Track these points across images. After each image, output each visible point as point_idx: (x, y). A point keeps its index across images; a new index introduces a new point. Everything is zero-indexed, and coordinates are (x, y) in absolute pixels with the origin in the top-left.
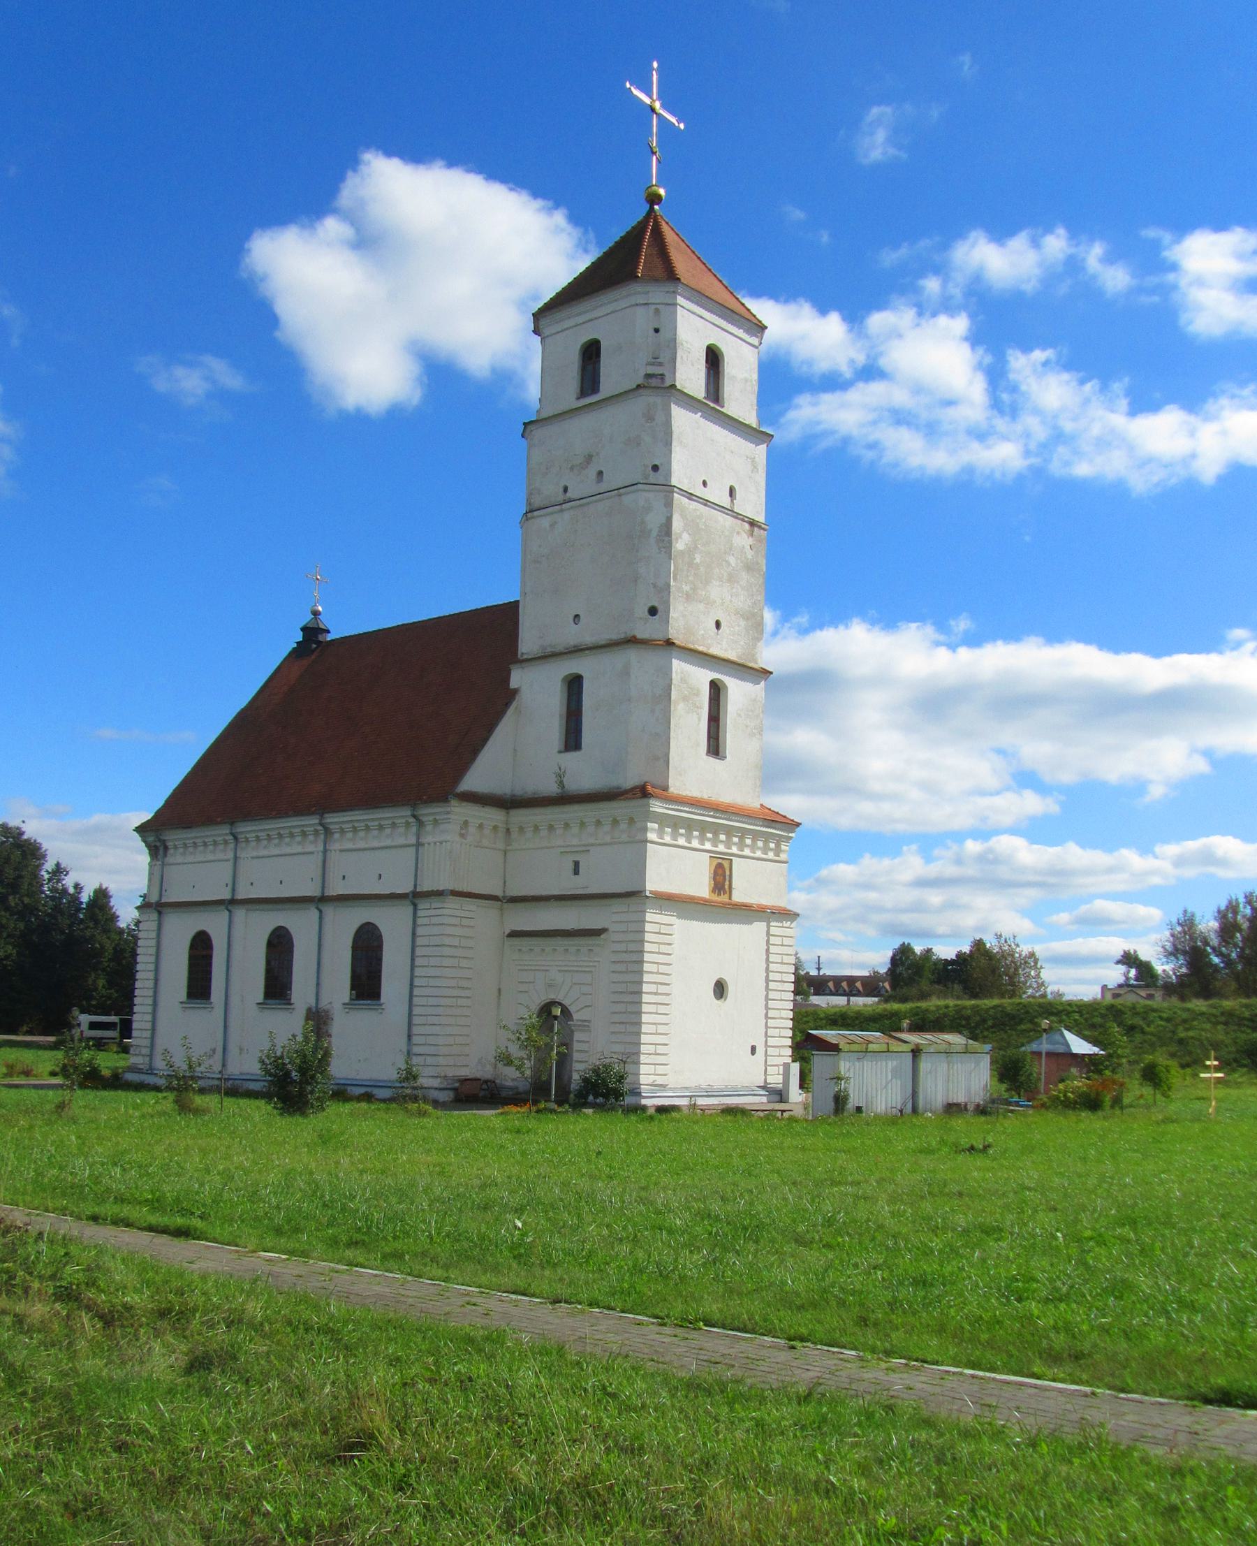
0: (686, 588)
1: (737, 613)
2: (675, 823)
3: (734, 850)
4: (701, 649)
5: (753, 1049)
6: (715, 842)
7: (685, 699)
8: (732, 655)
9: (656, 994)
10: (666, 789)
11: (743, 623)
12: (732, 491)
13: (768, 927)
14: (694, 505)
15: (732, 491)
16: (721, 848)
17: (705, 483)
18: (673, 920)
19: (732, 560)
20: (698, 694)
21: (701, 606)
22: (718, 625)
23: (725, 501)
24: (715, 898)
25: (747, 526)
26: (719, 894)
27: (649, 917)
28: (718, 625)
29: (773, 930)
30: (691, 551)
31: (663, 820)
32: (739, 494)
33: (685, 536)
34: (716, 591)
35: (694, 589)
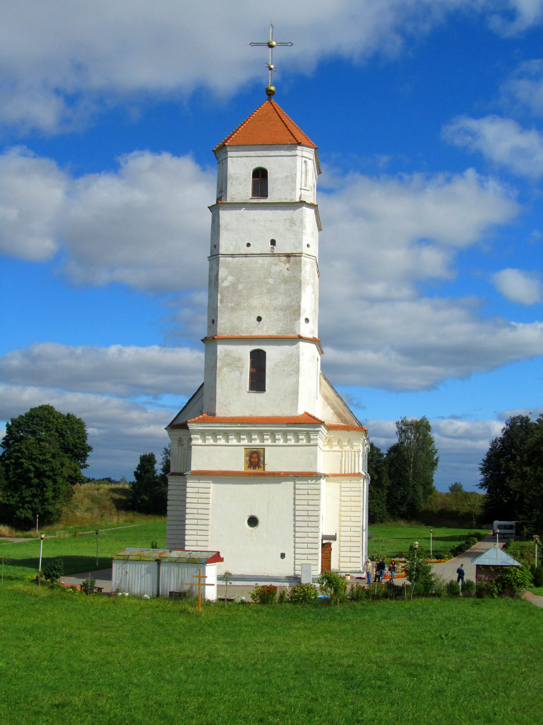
0: (230, 305)
1: (275, 309)
2: (214, 434)
3: (266, 443)
4: (245, 335)
5: (283, 556)
6: (251, 440)
7: (228, 365)
8: (273, 333)
9: (197, 525)
10: (214, 415)
11: (281, 313)
12: (273, 242)
13: (295, 484)
14: (236, 260)
15: (273, 242)
16: (257, 442)
17: (248, 245)
18: (212, 485)
19: (271, 281)
20: (240, 359)
21: (245, 312)
22: (259, 319)
23: (267, 248)
24: (251, 470)
25: (284, 258)
26: (254, 468)
27: (188, 485)
28: (259, 319)
29: (297, 486)
30: (234, 285)
31: (203, 434)
32: (277, 243)
33: (230, 278)
34: (255, 301)
35: (238, 304)
